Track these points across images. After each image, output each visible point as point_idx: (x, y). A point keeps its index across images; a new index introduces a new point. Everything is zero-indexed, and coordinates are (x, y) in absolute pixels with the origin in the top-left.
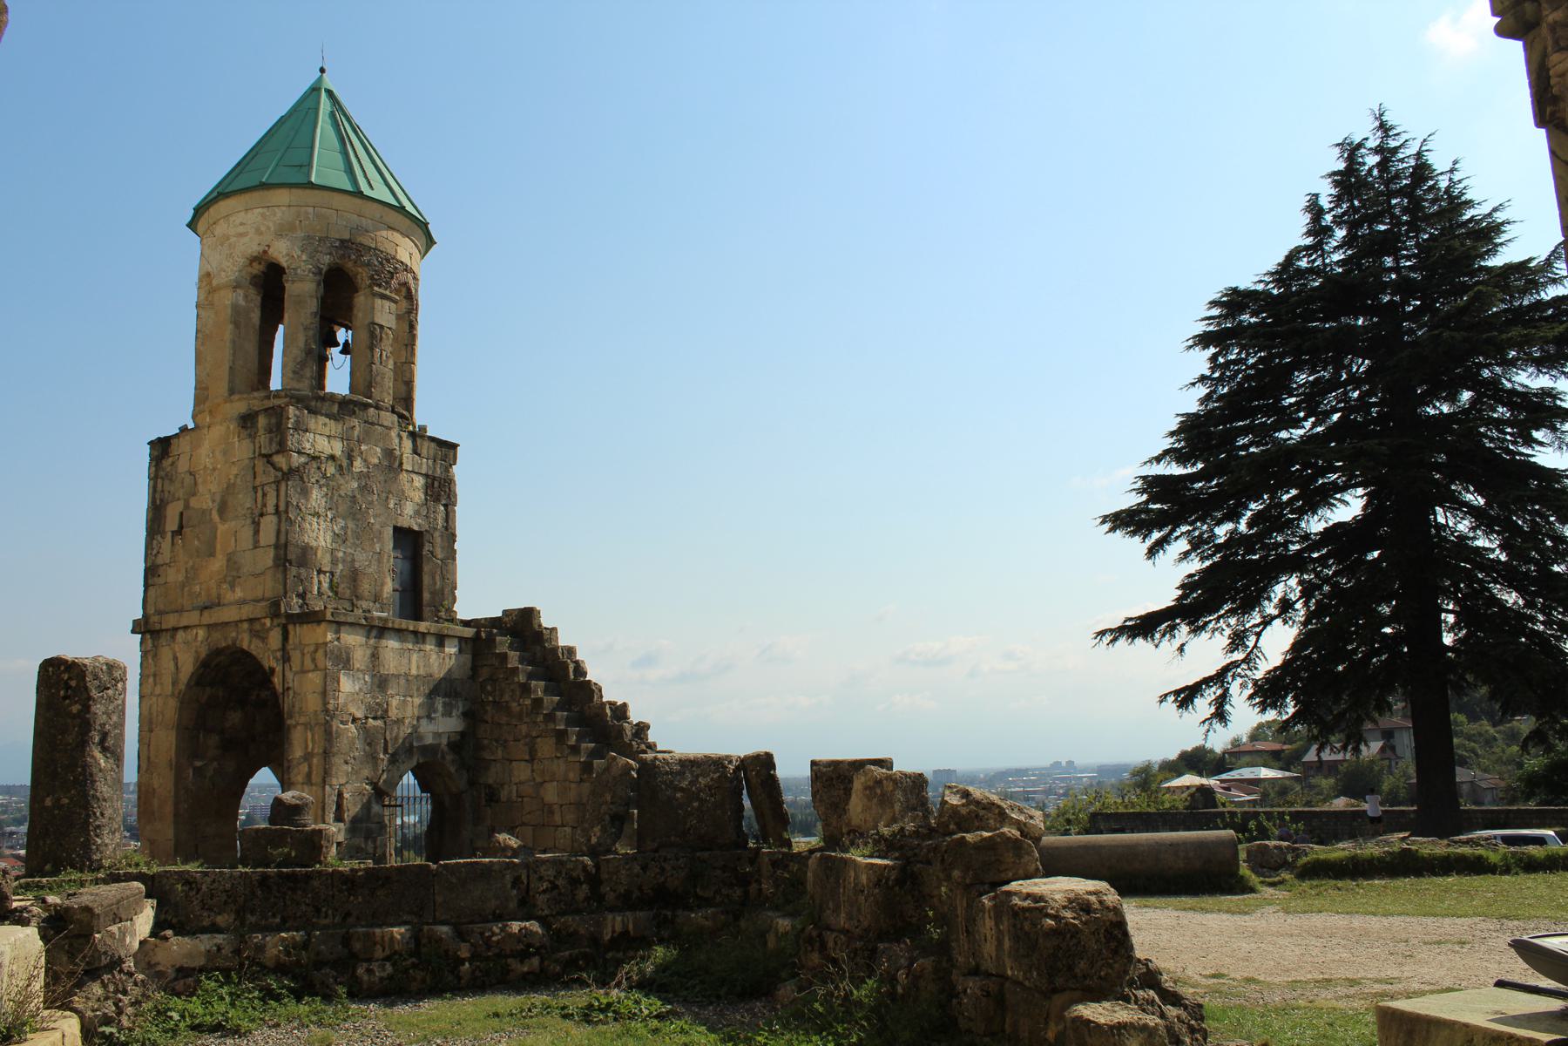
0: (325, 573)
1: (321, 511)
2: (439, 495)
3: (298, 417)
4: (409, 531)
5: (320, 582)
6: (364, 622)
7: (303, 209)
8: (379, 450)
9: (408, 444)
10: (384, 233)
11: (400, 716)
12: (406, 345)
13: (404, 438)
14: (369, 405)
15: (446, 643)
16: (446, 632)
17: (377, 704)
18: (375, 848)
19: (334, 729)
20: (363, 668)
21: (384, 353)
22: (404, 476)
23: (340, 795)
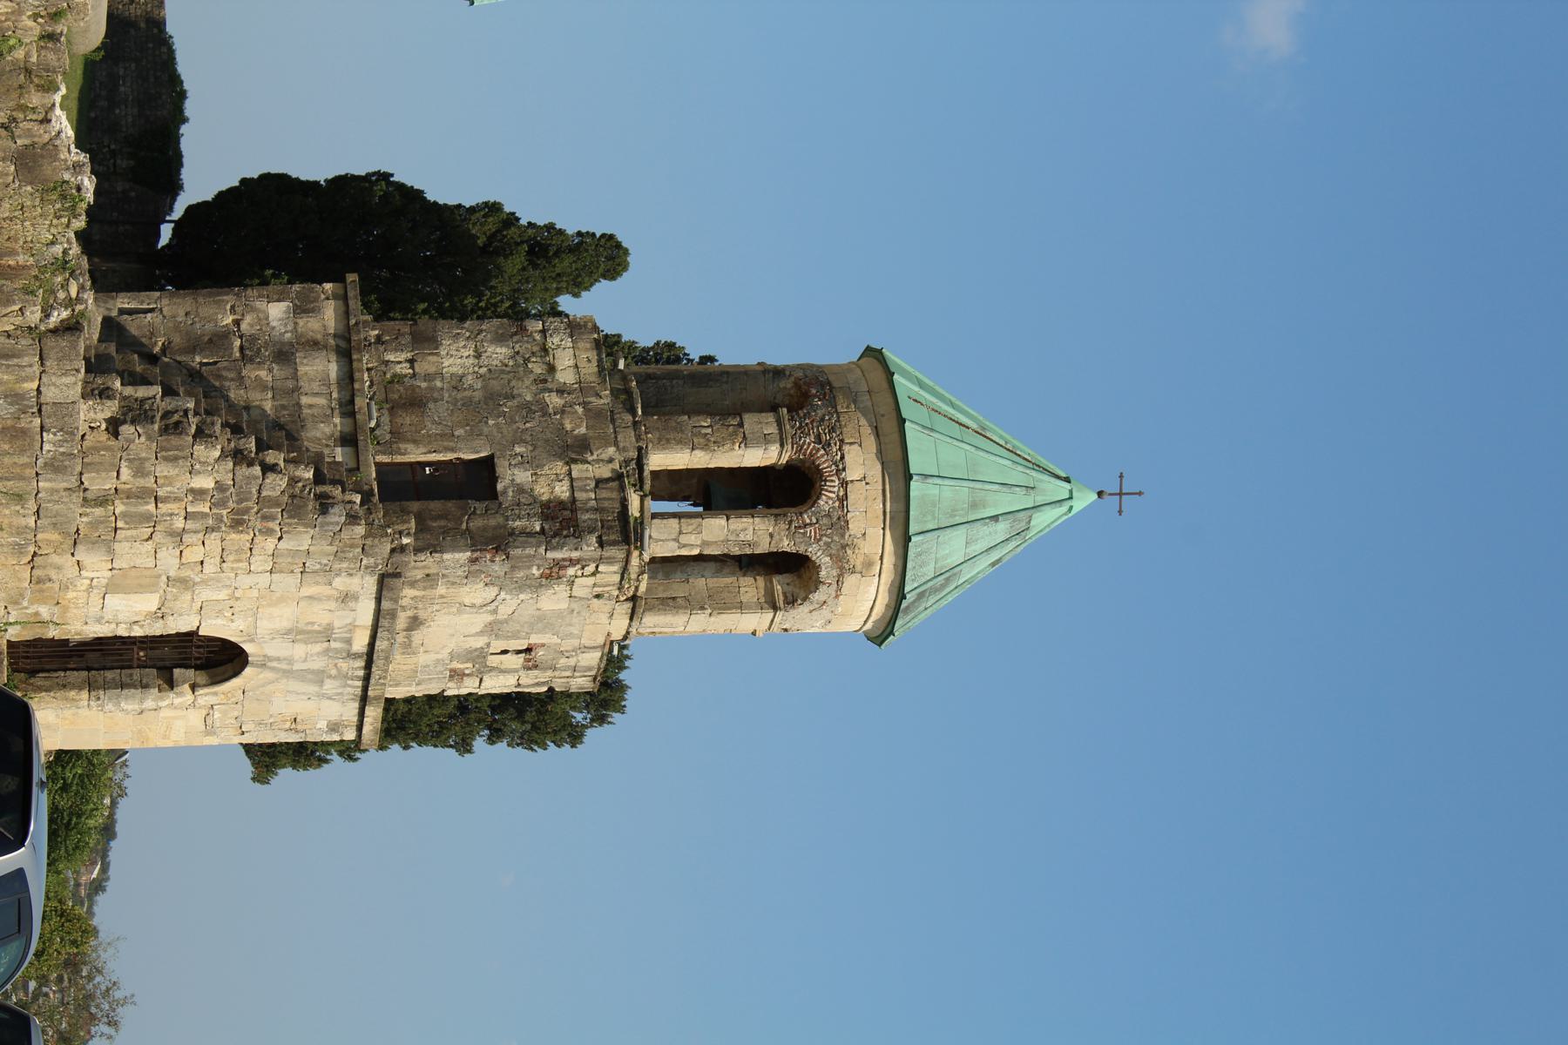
0: (412, 367)
1: (484, 360)
3: (585, 326)
4: (494, 479)
5: (400, 362)
6: (353, 322)
8: (583, 430)
9: (605, 472)
10: (863, 422)
11: (248, 382)
13: (610, 466)
14: (634, 413)
15: (347, 449)
16: (361, 444)
17: (259, 349)
19: (225, 298)
20: (300, 330)
21: (709, 430)
22: (560, 467)
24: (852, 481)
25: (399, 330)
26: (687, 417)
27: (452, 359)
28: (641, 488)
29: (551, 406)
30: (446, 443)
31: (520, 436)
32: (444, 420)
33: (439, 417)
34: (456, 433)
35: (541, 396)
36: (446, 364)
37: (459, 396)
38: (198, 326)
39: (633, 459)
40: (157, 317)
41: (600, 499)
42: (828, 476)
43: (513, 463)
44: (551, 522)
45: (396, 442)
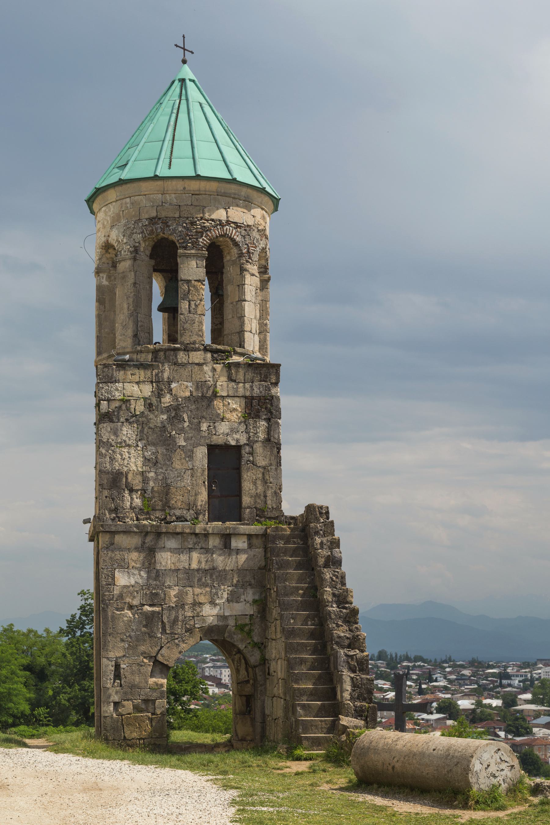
0: (137, 491)
2: (258, 411)
4: (226, 447)
7: (124, 201)
12: (239, 286)
18: (155, 709)
19: (110, 614)
20: (138, 565)
22: (218, 403)
23: (117, 667)
24: (227, 217)
25: (106, 497)
26: (182, 316)
27: (131, 464)
28: (228, 352)
29: (172, 403)
30: (199, 474)
31: (195, 425)
32: (180, 474)
33: (178, 477)
34: (191, 467)
35: (164, 409)
36: (135, 468)
37: (162, 462)
38: (133, 634)
39: (212, 356)
40: (124, 661)
41: (244, 380)
42: (224, 232)
43: (214, 432)
44: (261, 414)
45: (196, 507)
